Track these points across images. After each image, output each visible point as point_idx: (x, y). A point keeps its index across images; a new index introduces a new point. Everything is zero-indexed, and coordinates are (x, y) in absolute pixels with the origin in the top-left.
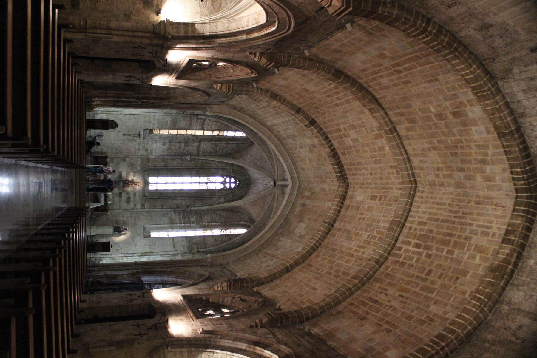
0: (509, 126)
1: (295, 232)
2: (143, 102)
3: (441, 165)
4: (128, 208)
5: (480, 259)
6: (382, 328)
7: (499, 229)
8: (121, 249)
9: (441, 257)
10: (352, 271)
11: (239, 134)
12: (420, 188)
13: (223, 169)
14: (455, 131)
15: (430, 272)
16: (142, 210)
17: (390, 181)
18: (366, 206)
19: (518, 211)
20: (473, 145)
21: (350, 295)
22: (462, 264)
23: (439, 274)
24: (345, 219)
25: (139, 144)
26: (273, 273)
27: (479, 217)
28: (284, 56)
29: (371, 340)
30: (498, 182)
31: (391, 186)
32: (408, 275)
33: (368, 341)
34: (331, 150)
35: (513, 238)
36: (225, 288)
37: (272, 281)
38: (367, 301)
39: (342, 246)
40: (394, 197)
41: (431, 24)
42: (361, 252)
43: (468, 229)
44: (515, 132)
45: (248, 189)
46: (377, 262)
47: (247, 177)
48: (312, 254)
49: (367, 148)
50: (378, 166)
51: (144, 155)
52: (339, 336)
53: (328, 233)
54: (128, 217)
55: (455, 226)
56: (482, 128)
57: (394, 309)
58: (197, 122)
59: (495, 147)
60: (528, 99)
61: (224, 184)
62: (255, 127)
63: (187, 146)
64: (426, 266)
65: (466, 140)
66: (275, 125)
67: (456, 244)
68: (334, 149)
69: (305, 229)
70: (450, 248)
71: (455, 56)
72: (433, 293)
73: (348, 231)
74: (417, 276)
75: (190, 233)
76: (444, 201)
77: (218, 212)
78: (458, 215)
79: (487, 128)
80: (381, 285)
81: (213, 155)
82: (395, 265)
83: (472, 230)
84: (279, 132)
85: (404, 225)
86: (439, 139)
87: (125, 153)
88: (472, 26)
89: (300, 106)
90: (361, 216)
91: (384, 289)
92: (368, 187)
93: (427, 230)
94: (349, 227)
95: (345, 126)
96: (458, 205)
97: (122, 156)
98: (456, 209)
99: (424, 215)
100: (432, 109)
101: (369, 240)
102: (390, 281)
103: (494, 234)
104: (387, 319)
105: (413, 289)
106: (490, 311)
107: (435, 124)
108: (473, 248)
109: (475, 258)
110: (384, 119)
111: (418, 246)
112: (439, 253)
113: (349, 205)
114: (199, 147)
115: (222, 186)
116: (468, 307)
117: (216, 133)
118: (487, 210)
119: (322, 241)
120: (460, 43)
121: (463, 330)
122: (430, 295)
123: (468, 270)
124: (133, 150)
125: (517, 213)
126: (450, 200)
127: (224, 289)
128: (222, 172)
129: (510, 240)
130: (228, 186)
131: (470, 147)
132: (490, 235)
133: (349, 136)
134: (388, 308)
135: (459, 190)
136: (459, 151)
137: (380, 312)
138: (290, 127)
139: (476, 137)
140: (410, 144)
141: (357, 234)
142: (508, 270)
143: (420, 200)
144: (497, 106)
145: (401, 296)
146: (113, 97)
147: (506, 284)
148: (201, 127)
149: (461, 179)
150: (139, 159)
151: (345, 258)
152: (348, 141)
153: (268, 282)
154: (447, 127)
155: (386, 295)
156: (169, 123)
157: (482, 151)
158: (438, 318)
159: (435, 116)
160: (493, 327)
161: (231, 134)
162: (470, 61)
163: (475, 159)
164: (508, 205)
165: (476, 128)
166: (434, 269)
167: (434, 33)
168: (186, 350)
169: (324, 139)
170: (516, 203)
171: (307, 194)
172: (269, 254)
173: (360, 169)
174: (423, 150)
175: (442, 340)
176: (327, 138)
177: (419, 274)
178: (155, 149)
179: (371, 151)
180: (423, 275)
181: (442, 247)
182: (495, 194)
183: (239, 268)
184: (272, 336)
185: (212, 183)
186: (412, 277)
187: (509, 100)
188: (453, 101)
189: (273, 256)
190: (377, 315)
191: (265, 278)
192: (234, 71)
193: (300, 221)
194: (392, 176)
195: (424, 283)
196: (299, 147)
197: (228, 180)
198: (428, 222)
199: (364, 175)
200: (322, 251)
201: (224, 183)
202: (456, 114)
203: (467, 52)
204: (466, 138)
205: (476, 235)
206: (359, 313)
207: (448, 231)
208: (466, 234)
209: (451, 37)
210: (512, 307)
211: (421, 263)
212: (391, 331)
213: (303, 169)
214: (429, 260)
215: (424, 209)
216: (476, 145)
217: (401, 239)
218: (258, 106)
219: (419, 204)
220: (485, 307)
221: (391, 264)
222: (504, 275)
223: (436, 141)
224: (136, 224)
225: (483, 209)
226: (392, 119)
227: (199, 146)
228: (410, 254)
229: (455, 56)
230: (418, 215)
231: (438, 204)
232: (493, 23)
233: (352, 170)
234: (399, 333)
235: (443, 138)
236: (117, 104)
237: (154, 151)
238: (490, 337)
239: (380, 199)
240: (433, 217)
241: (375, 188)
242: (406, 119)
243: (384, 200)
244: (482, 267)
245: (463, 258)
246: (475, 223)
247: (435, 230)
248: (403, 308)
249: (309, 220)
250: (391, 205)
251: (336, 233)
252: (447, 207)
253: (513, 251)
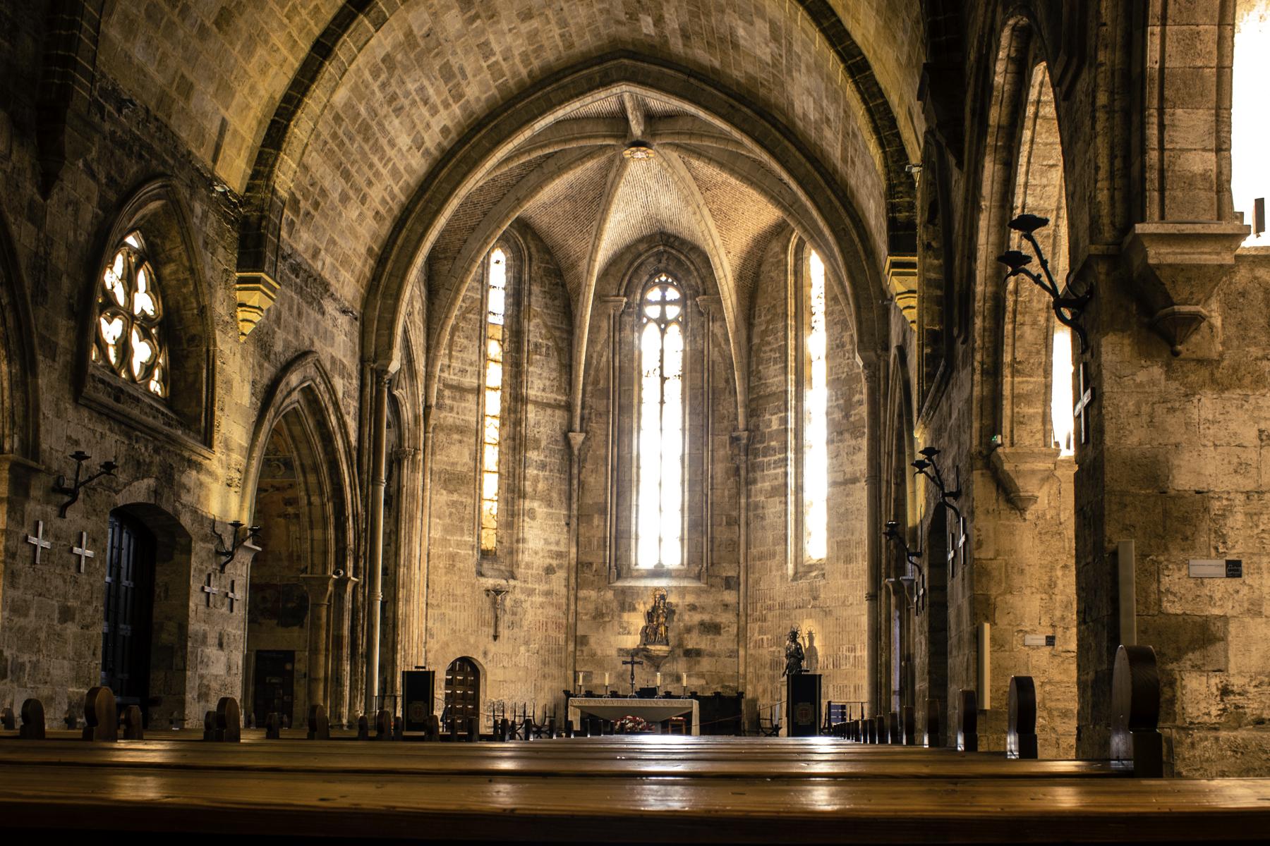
2: (356, 568)
4: (734, 630)
8: (854, 650)
13: (618, 326)
16: (742, 586)
25: (531, 592)
36: (913, 282)
47: (642, 247)
51: (568, 579)
54: (760, 632)
58: (451, 409)
61: (667, 323)
62: (438, 212)
63: (537, 441)
66: (418, 144)
75: (817, 431)
77: (756, 341)
81: (571, 358)
84: (445, 131)
87: (562, 637)
97: (571, 647)
115: (674, 330)
117: (494, 349)
124: (551, 611)
127: (915, 287)
128: (628, 331)
130: (673, 312)
138: (412, 87)
146: (338, 660)
148: (471, 398)
150: (582, 593)
156: (455, 497)
161: (497, 302)
168: (1007, 380)
172: (845, 149)
178: (547, 542)
185: (661, 360)
192: (170, 260)
193: (736, 46)
196: (486, 58)
197: (653, 311)
201: (663, 322)
218: (345, 198)
224: (782, 606)
227: (536, 403)
236: (361, 649)
237: (554, 548)
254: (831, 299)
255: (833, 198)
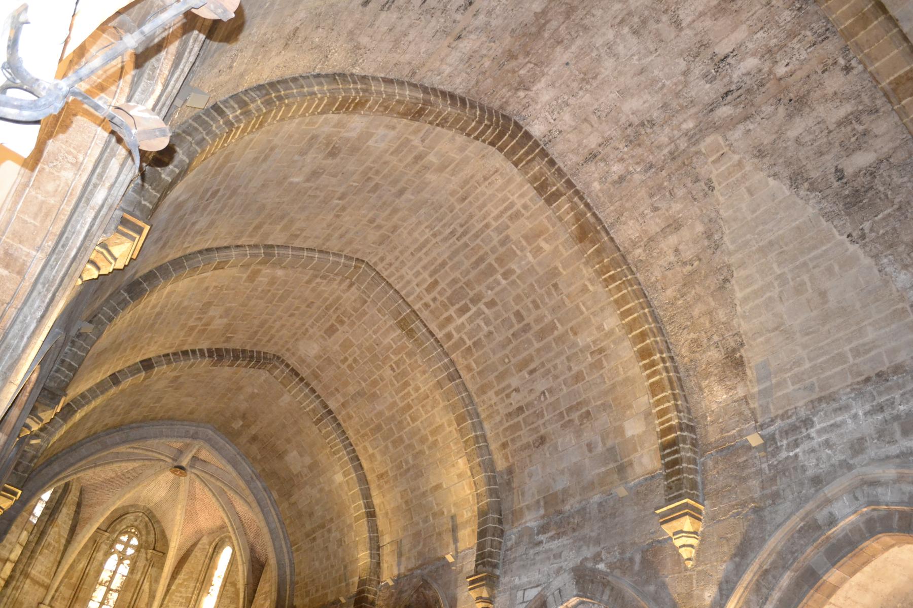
0: (417, 98)
1: (295, 473)
3: (371, 215)
5: (547, 242)
6: (577, 422)
7: (522, 196)
9: (504, 289)
10: (438, 419)
11: (46, 496)
12: (372, 260)
14: (350, 167)
15: (518, 315)
17: (326, 295)
18: (337, 347)
19: (520, 160)
20: (387, 157)
21: (486, 441)
22: (537, 268)
23: (531, 306)
24: (333, 389)
26: (368, 540)
27: (485, 209)
28: (58, 371)
29: (590, 447)
30: (458, 157)
31: (334, 296)
32: (503, 346)
33: (590, 451)
34: (209, 356)
35: (554, 189)
37: (379, 548)
38: (512, 422)
39: (380, 414)
40: (355, 300)
41: (225, 109)
42: (412, 392)
43: (492, 233)
44: (427, 97)
45: (154, 516)
46: (451, 378)
48: (360, 465)
49: (252, 303)
50: (290, 299)
52: (559, 487)
53: (339, 425)
55: (472, 246)
56: (381, 131)
57: (550, 391)
59: (415, 132)
60: (405, 52)
64: (506, 316)
65: (374, 162)
66: (91, 428)
67: (500, 260)
68: (209, 350)
69: (301, 456)
70: (502, 271)
71: (287, 105)
72: (554, 328)
73: (358, 393)
74: (513, 335)
76: (422, 240)
77: (173, 587)
78: (458, 235)
79: (387, 126)
80: (496, 389)
82: (472, 355)
83: (497, 229)
85: (414, 311)
86: (338, 195)
88: (273, 53)
89: (109, 373)
90: (347, 364)
91: (504, 389)
92: (307, 330)
93: (447, 285)
94: (352, 389)
95: (195, 316)
96: (444, 225)
98: (449, 231)
99: (421, 277)
100: (296, 180)
101: (398, 371)
102: (496, 374)
103: (525, 207)
104: (563, 409)
105: (532, 351)
106: (632, 273)
107: (316, 189)
108: (524, 243)
109: (541, 248)
110: (246, 255)
111: (463, 310)
112: (497, 289)
113: (314, 370)
114: (35, 582)
115: (127, 562)
116: (616, 297)
118: (483, 194)
119: (347, 438)
120: (272, 85)
121: (647, 321)
122: (556, 333)
123: (552, 265)
125: (524, 162)
126: (427, 230)
129: (553, 194)
130: (130, 551)
131: (385, 163)
132: (523, 211)
133: (212, 318)
134: (542, 399)
135: (422, 211)
136: (377, 179)
137: (545, 412)
139: (382, 146)
140: (306, 238)
141: (374, 383)
142: (592, 220)
143: (392, 269)
144: (384, 96)
145: (531, 372)
147: (608, 233)
149: (411, 200)
151: (406, 419)
152: (219, 323)
153: (379, 555)
154: (335, 176)
155: (517, 390)
157: (405, 150)
158: (602, 341)
159: (308, 180)
160: (657, 281)
162: (306, 89)
163: (406, 167)
164: (498, 165)
165: (373, 139)
166: (517, 308)
167: (241, 114)
169: (185, 360)
170: (508, 156)
171: (237, 424)
173: (271, 327)
174: (329, 225)
175: (650, 355)
176: (185, 353)
177: (511, 331)
179: (261, 298)
180: (517, 327)
181: (491, 280)
182: (468, 171)
183: (317, 591)
184: (520, 593)
186: (510, 342)
187: (383, 75)
188: (316, 146)
189: (322, 526)
190: (547, 418)
191: (371, 557)
193: (281, 456)
194: (322, 288)
195: (532, 332)
197: (119, 547)
198: (436, 276)
199: (283, 326)
200: (365, 448)
202: (333, 154)
203: (291, 84)
204: (371, 159)
205: (508, 227)
206: (528, 443)
207: (474, 259)
208: (496, 239)
209: (258, 93)
210: (642, 243)
211: (496, 319)
212: (588, 413)
213: (191, 413)
214: (499, 307)
215: (411, 273)
216: (392, 154)
217: (433, 327)
219: (397, 275)
220: (626, 276)
221: (466, 359)
222: (596, 228)
223: (337, 201)
225: (478, 199)
226: (252, 243)
227: (32, 579)
228: (468, 327)
229: (287, 105)
230: (414, 284)
231: (420, 249)
232: (298, 25)
233: (261, 340)
234: (599, 403)
235: (341, 190)
238: (670, 292)
239: (342, 322)
240: (433, 267)
241: (317, 320)
242: (270, 224)
243: (349, 318)
244: (561, 247)
245: (529, 262)
246: (489, 219)
247: (457, 274)
248: (556, 377)
249: (289, 443)
250: (365, 313)
251: (348, 414)
252: (434, 241)
253: (570, 200)
254: (228, 580)
255: (284, 546)
